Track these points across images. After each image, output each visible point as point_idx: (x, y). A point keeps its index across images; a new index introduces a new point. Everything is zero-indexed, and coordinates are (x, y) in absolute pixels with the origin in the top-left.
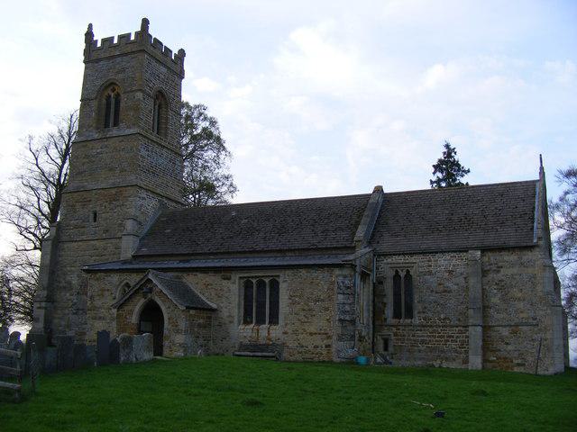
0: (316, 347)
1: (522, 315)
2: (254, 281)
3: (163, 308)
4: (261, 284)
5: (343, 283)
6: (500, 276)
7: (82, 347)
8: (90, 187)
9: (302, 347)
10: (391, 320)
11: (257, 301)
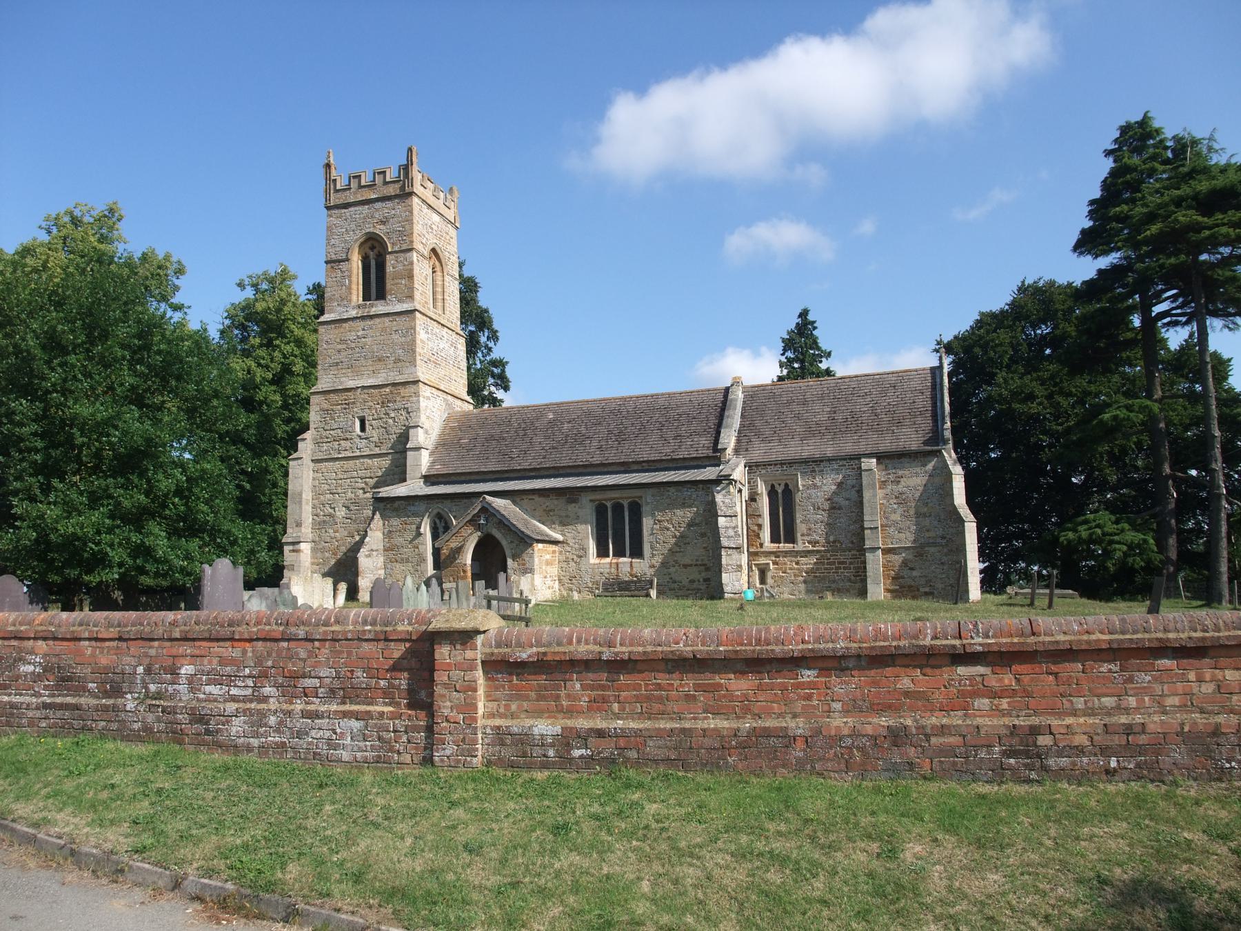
0: (692, 581)
1: (927, 535)
2: (625, 503)
3: (504, 543)
4: (618, 508)
5: (724, 502)
6: (900, 488)
7: (1227, 378)
8: (351, 384)
9: (675, 582)
10: (768, 545)
11: (614, 529)
